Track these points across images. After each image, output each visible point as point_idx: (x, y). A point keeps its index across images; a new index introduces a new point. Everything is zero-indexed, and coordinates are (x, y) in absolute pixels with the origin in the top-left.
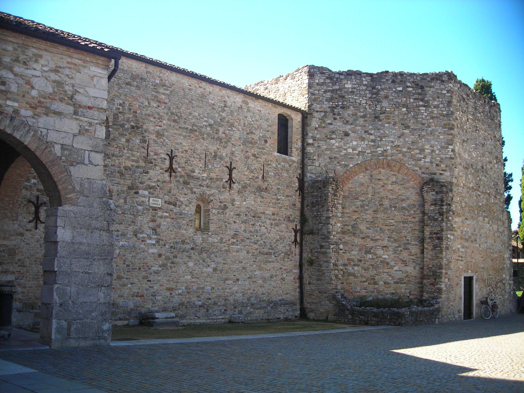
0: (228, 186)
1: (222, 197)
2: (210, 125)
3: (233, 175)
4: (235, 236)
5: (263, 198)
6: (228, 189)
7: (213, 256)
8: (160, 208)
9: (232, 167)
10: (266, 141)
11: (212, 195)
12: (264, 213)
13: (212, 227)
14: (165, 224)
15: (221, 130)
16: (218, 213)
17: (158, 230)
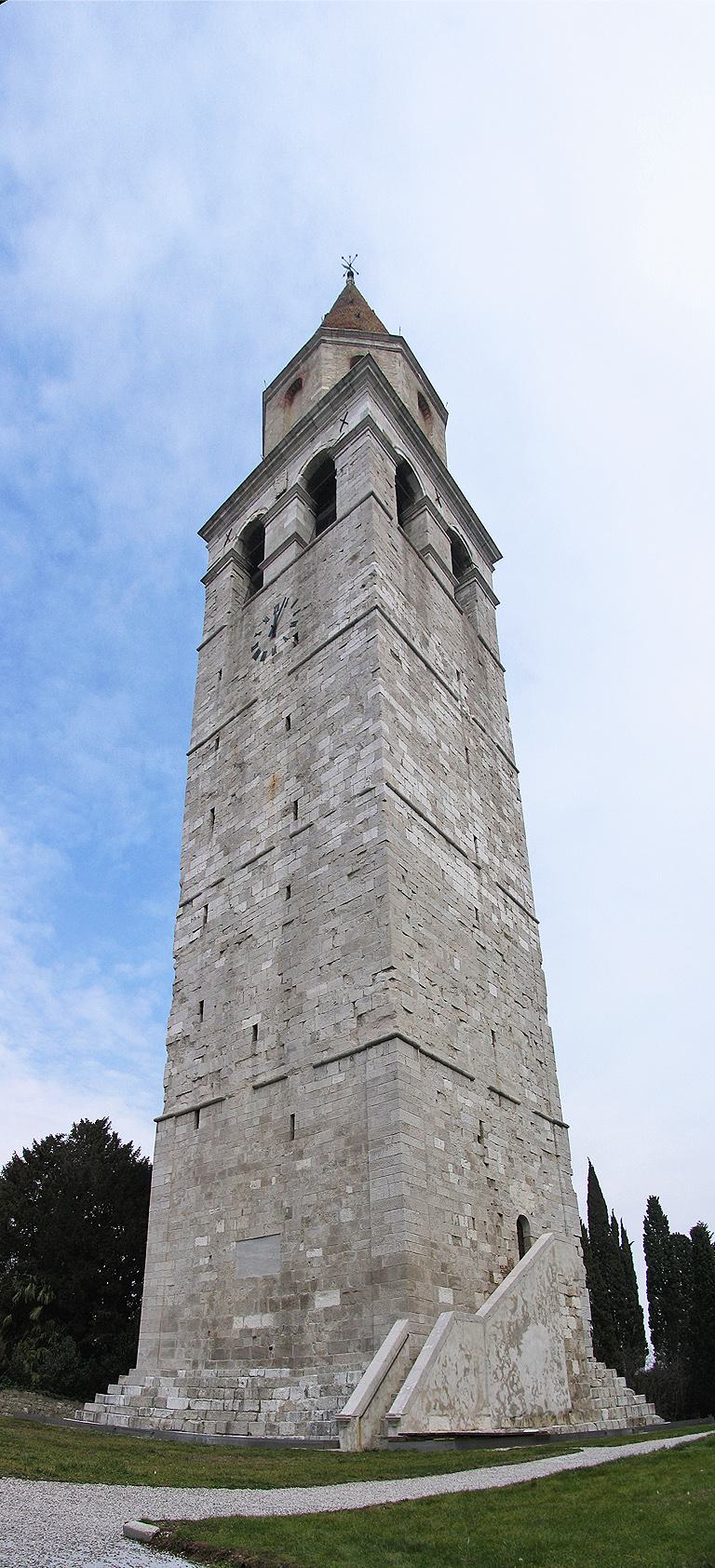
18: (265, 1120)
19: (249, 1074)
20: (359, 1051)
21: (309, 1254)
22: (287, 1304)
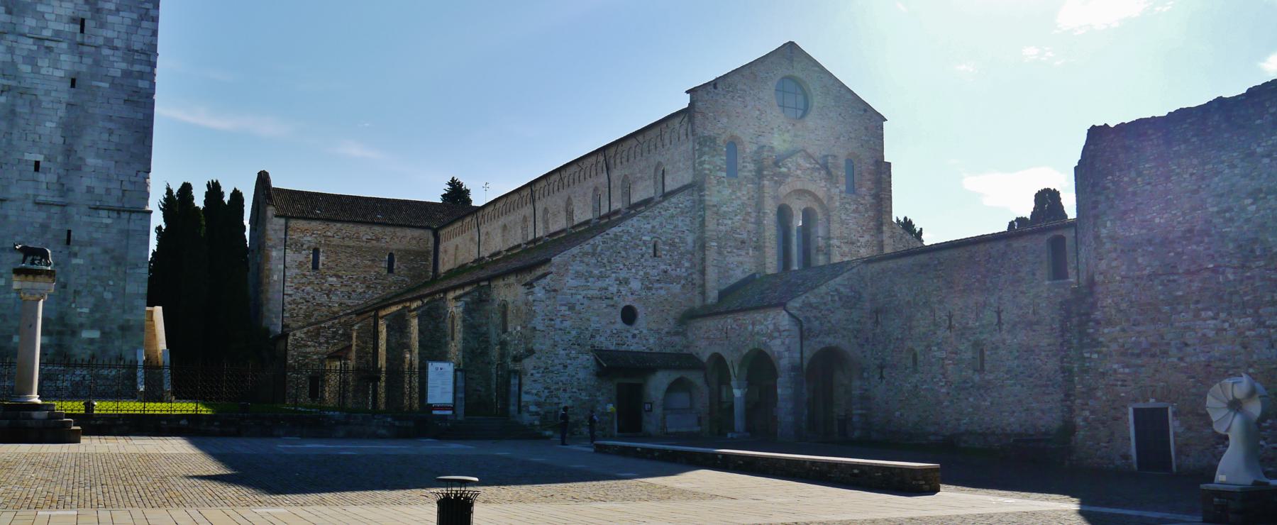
0: (997, 328)
1: (993, 339)
2: (978, 280)
3: (1002, 317)
4: (1008, 372)
5: (1034, 331)
6: (998, 331)
7: (989, 391)
8: (946, 358)
9: (1000, 310)
10: (1034, 274)
11: (985, 339)
12: (1038, 346)
13: (987, 367)
14: (950, 368)
15: (988, 281)
16: (992, 354)
17: (946, 375)
18: (44, 227)
19: (31, 192)
20: (124, 211)
21: (79, 310)
22: (61, 333)
